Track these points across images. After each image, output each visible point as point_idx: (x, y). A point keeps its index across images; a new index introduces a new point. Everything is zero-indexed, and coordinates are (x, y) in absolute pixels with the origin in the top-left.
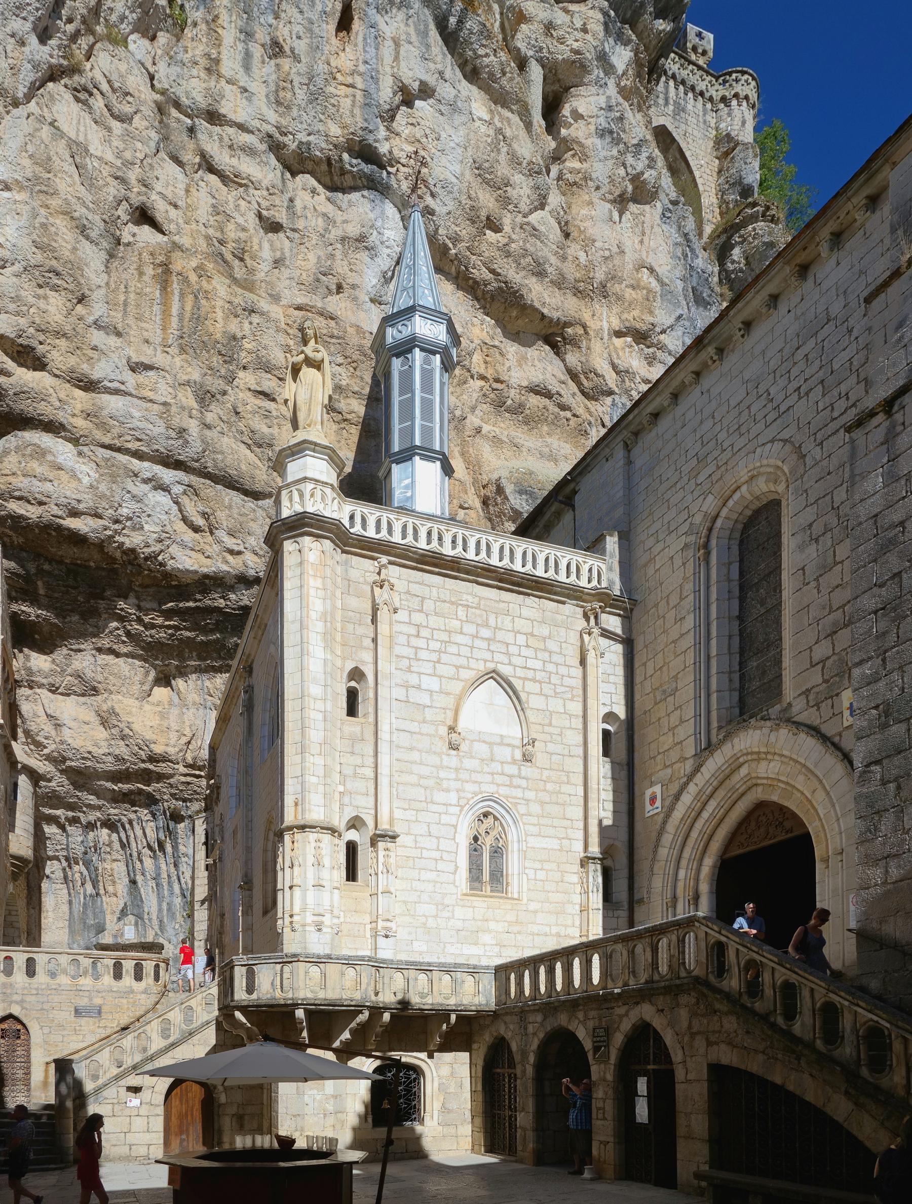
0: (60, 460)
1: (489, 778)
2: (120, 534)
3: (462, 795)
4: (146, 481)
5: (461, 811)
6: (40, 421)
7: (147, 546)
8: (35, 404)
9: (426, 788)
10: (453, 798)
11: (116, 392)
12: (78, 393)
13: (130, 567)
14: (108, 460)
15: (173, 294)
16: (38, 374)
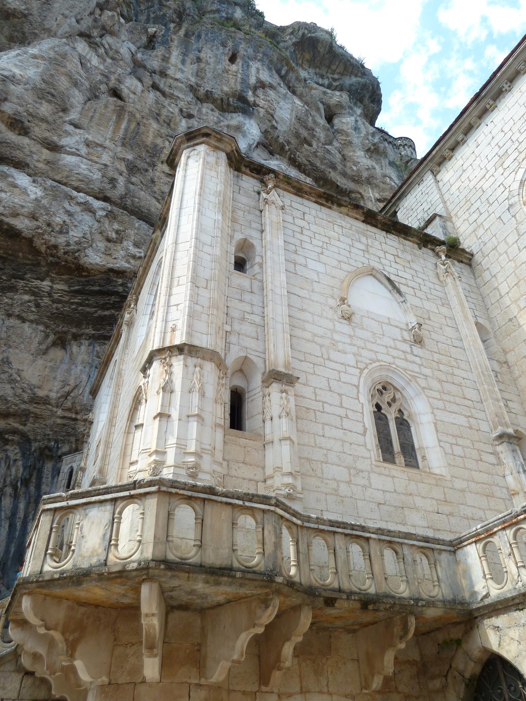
0: (19, 182)
1: (384, 350)
2: (49, 234)
3: (360, 359)
4: (79, 204)
5: (361, 373)
6: (12, 160)
7: (68, 244)
8: (12, 151)
9: (321, 346)
10: (351, 360)
11: (73, 154)
12: (45, 151)
13: (51, 259)
14: (55, 187)
15: (123, 119)
16: (21, 137)
